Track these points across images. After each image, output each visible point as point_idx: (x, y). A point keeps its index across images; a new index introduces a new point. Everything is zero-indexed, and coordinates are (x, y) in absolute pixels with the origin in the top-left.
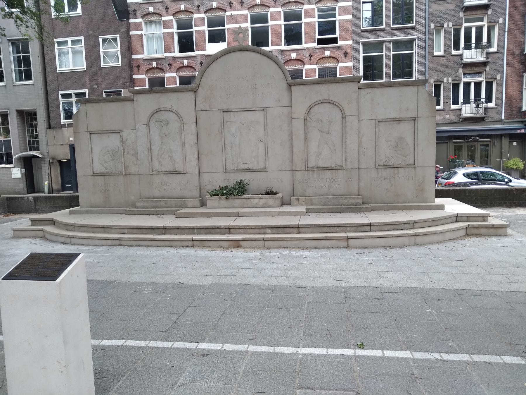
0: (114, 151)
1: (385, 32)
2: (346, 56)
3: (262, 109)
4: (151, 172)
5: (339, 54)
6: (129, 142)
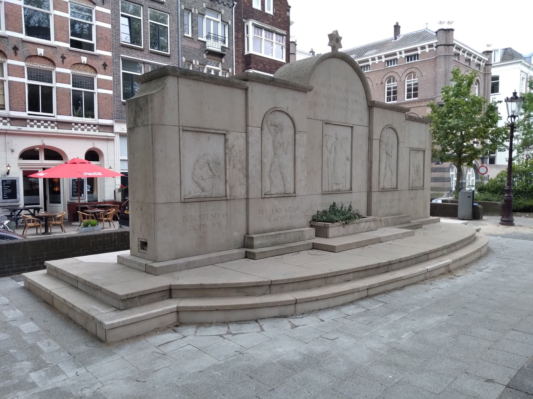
0: (216, 162)
1: (144, 53)
2: (105, 68)
3: (352, 125)
4: (263, 194)
5: (99, 65)
6: (235, 150)
